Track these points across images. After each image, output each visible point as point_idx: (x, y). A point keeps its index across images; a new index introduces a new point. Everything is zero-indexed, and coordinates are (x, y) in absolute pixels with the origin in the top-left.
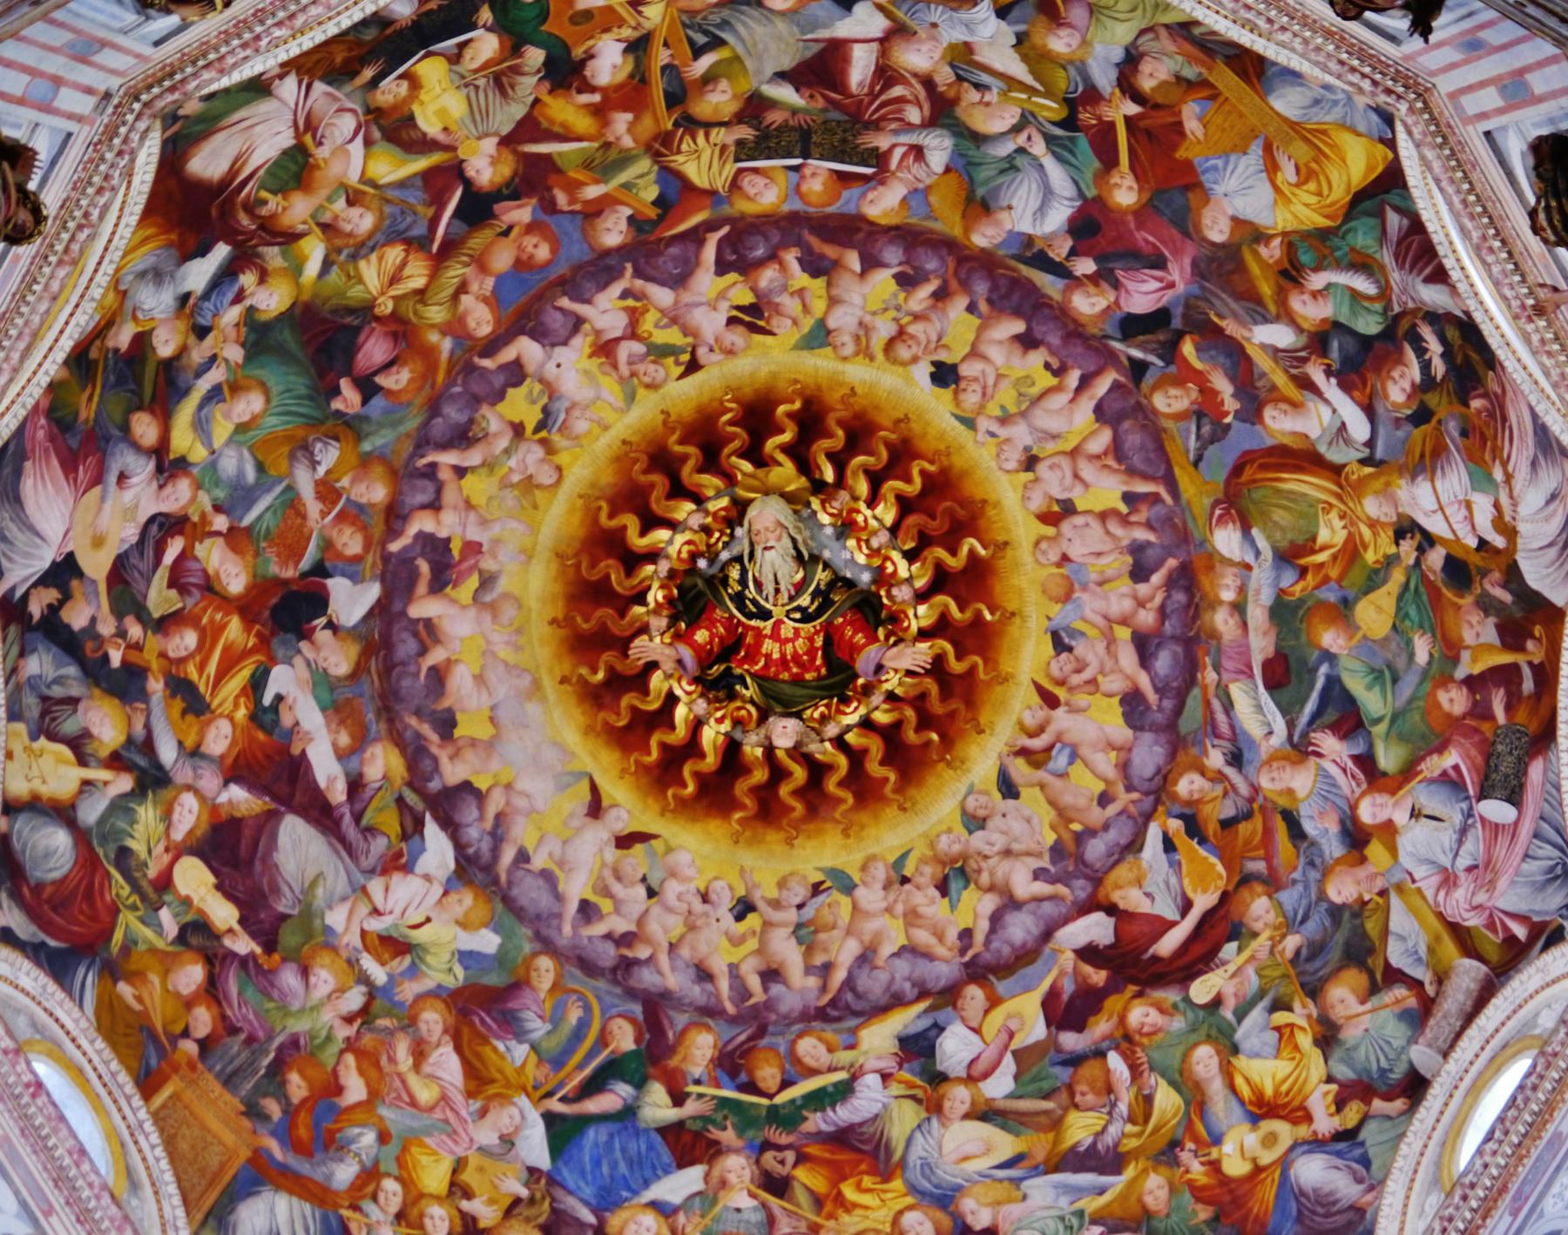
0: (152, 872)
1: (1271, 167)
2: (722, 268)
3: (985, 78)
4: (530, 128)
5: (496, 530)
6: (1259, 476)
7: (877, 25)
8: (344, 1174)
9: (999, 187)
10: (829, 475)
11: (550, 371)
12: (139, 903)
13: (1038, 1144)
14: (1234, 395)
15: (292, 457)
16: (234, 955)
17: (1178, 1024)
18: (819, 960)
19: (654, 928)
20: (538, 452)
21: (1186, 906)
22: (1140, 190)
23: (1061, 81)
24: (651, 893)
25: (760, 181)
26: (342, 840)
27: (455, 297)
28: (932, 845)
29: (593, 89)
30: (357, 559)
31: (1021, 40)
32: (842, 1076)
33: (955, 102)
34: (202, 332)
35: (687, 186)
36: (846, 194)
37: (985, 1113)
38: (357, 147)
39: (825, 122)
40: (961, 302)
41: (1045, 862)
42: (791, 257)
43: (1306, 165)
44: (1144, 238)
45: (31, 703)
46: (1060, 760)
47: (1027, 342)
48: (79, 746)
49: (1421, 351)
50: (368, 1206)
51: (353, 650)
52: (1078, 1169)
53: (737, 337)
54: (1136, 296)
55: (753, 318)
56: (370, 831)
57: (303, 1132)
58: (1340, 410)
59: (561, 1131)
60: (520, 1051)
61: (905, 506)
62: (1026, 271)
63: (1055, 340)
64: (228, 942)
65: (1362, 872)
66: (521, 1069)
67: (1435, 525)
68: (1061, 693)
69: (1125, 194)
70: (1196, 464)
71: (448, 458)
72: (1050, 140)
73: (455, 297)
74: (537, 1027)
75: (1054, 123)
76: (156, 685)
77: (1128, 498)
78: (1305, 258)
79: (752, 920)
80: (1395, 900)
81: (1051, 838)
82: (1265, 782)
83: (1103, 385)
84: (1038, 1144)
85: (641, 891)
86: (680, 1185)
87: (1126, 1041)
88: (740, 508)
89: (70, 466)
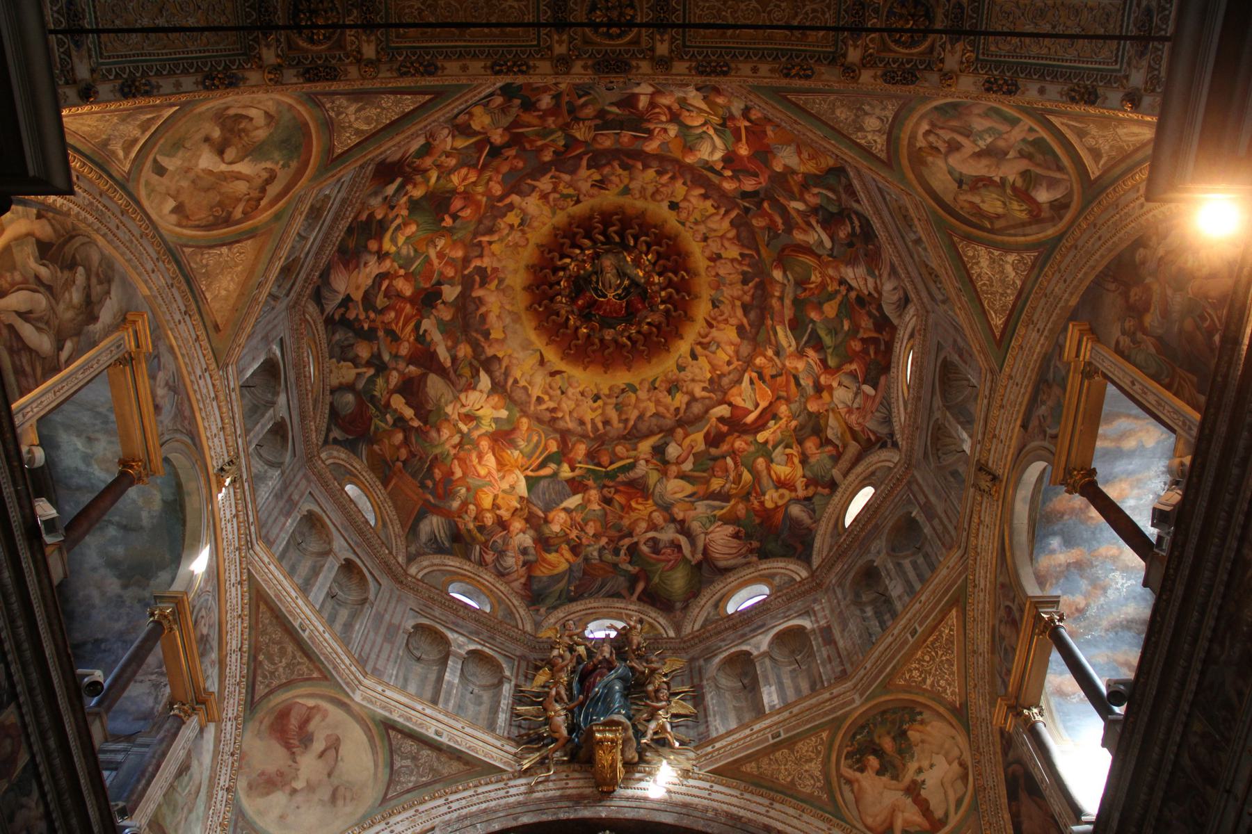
1: (799, 153)
2: (589, 167)
4: (516, 123)
5: (504, 263)
7: (650, 90)
8: (456, 504)
10: (632, 243)
11: (524, 205)
13: (701, 489)
15: (427, 245)
17: (752, 449)
18: (624, 417)
19: (564, 406)
20: (520, 234)
21: (757, 405)
23: (720, 112)
24: (563, 393)
26: (450, 380)
27: (487, 183)
28: (666, 376)
29: (539, 110)
30: (453, 278)
31: (705, 98)
32: (631, 460)
33: (680, 115)
34: (392, 208)
35: (576, 139)
37: (682, 476)
38: (449, 139)
40: (680, 181)
41: (706, 385)
42: (616, 164)
44: (752, 166)
45: (337, 349)
46: (714, 348)
47: (705, 197)
48: (355, 362)
49: (852, 223)
50: (466, 517)
51: (452, 311)
52: (714, 499)
53: (595, 191)
55: (601, 184)
56: (460, 376)
57: (440, 491)
59: (531, 482)
60: (516, 453)
61: (659, 255)
62: (705, 172)
63: (716, 197)
65: (820, 402)
66: (516, 461)
67: (854, 284)
68: (714, 323)
69: (744, 151)
70: (768, 245)
71: (485, 239)
72: (715, 130)
73: (487, 183)
74: (522, 444)
76: (381, 334)
77: (742, 255)
78: (811, 183)
79: (600, 403)
80: (831, 414)
81: (709, 376)
82: (787, 363)
83: (733, 214)
84: (701, 489)
85: (559, 392)
86: (574, 501)
87: (734, 453)
88: (596, 256)
89: (346, 265)
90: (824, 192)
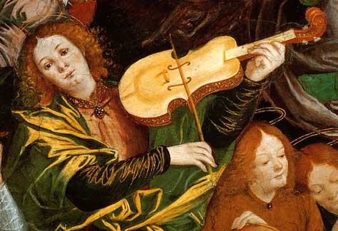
0: (119, 151)
12: (147, 192)
16: (278, 71)
64: (257, 75)
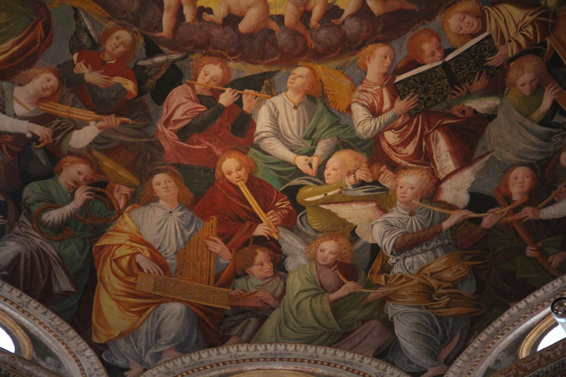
3: (360, 192)
6: (32, 34)
9: (310, 120)
14: (82, 75)
22: (223, 177)
25: (466, 30)
31: (354, 236)
33: (370, 164)
36: (405, 53)
39: (445, 97)
40: (289, 19)
43: (136, 276)
54: (184, 100)
58: (11, 119)
62: (261, 69)
63: (216, 32)
72: (298, 173)
75: (301, 186)
78: (98, 205)
90: (68, 209)
